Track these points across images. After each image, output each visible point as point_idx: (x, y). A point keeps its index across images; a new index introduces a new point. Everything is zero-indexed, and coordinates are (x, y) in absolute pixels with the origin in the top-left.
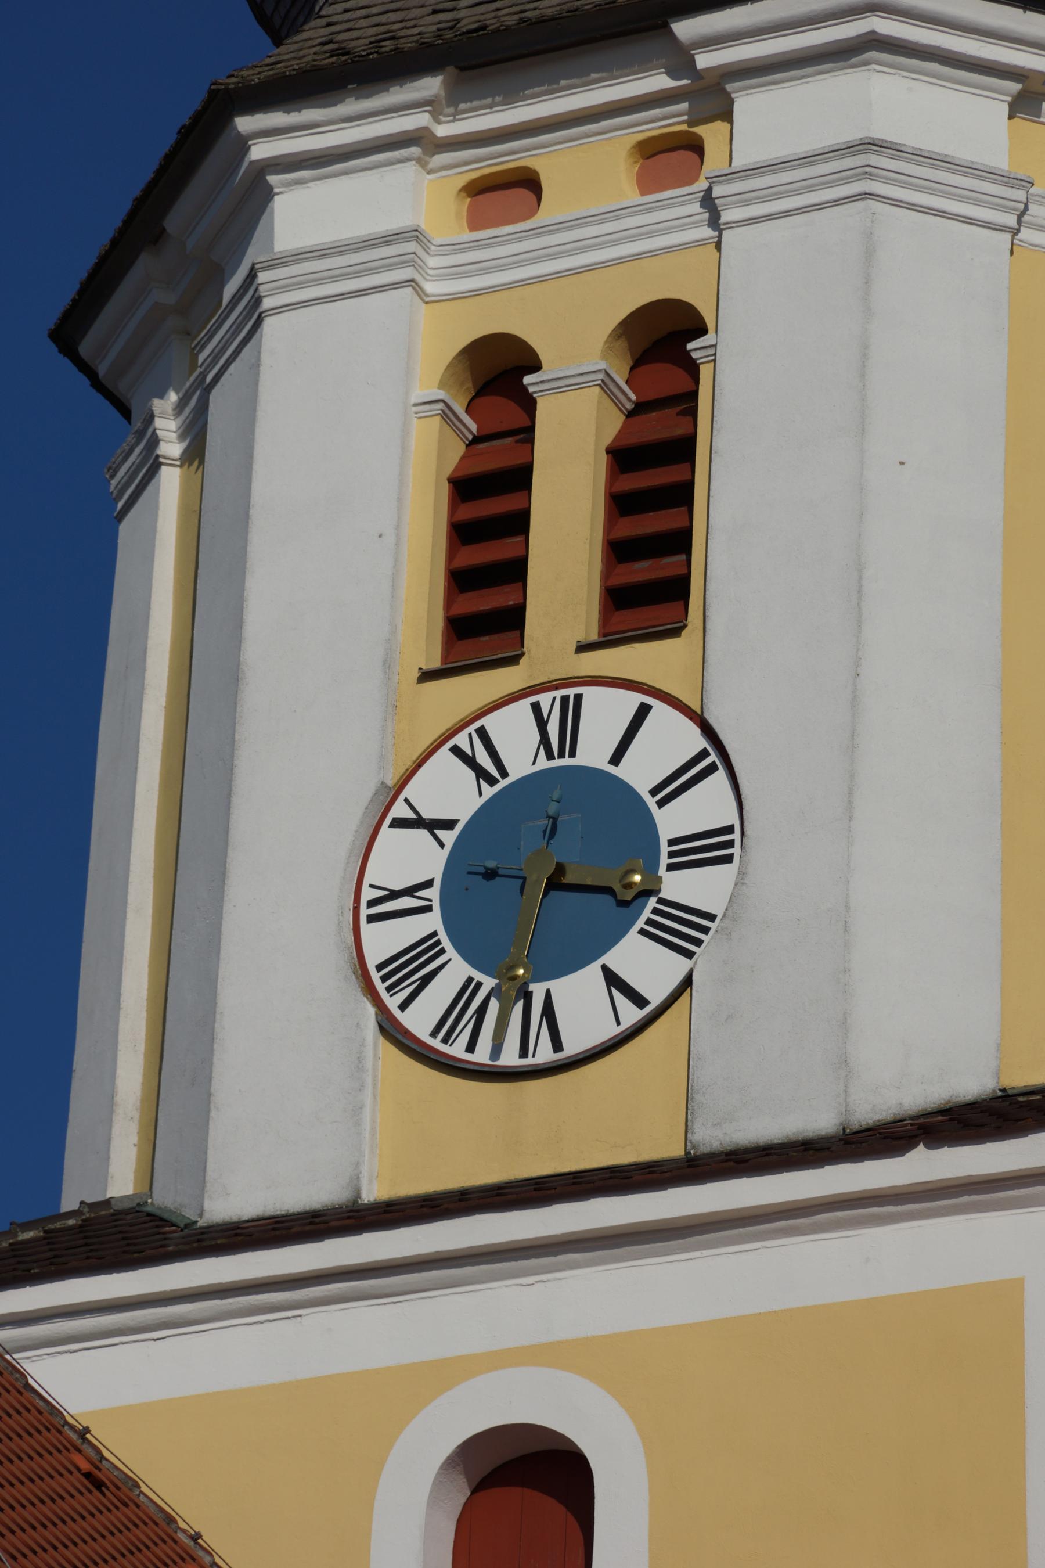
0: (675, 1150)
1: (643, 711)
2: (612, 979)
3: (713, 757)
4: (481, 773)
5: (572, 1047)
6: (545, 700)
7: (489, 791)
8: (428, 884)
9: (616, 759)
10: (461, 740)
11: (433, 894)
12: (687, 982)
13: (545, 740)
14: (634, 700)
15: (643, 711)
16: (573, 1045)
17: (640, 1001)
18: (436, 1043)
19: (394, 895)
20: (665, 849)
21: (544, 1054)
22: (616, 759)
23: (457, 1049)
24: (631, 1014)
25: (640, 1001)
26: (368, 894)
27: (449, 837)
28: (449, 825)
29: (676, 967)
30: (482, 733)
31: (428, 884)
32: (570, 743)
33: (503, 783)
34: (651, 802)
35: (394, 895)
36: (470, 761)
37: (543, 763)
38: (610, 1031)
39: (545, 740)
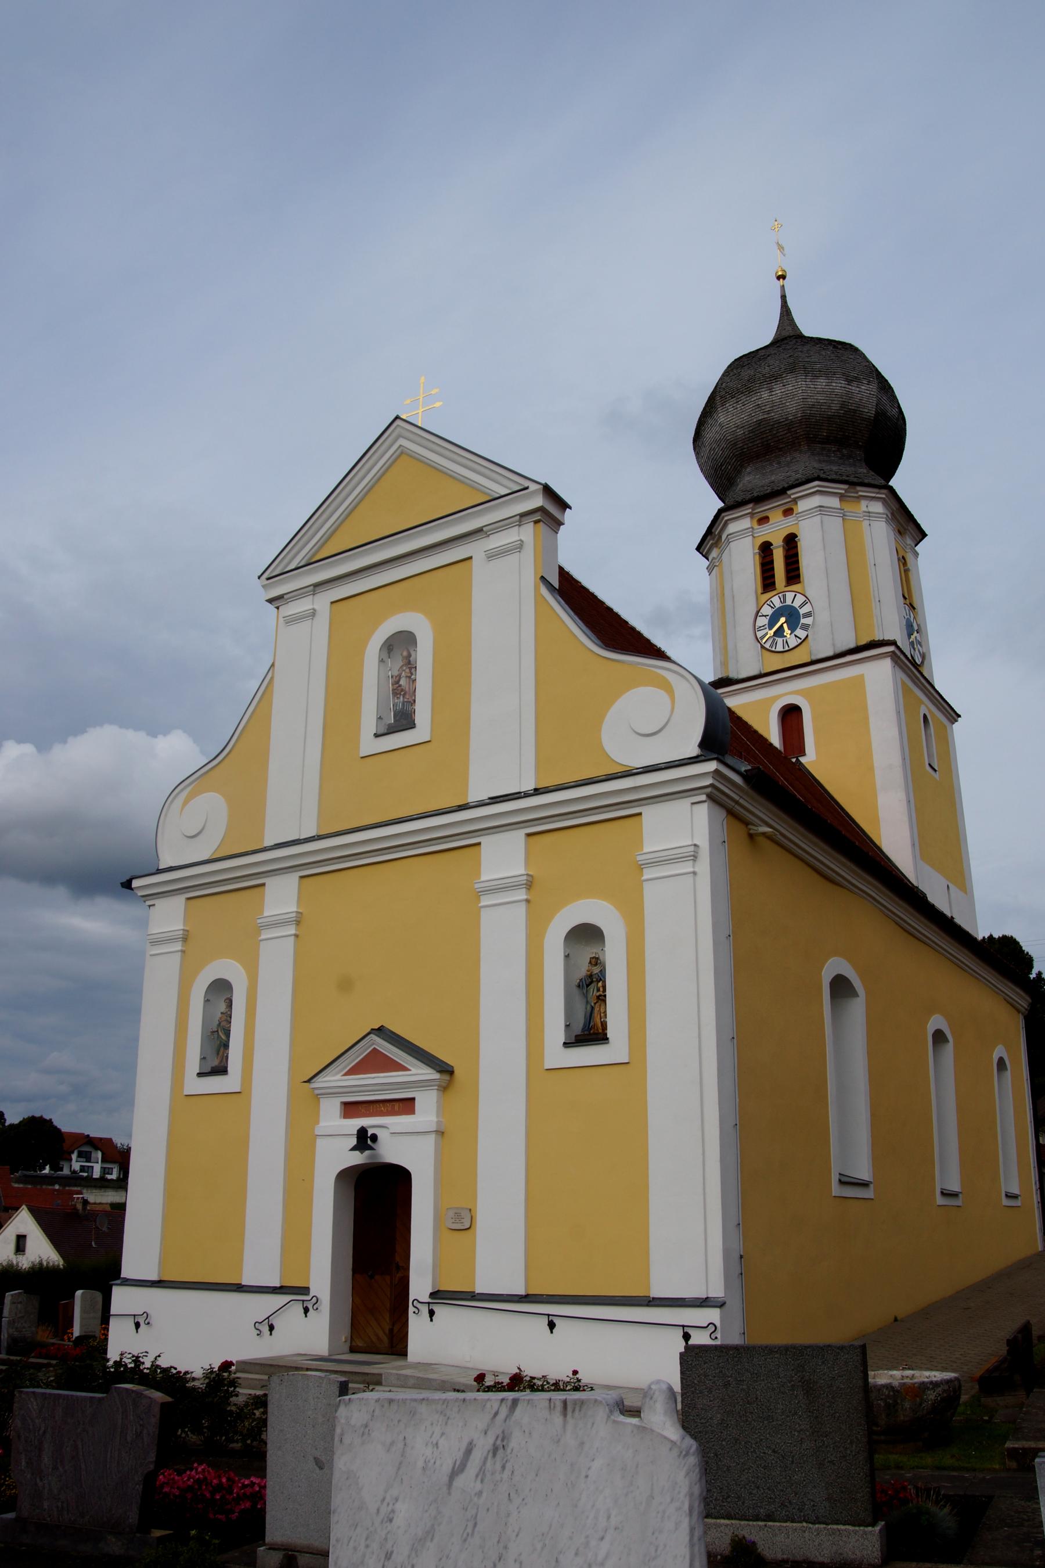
0: (809, 660)
1: (796, 595)
2: (796, 636)
3: (807, 601)
4: (772, 607)
5: (791, 647)
6: (780, 595)
7: (773, 610)
8: (766, 625)
9: (792, 603)
10: (768, 602)
11: (767, 626)
12: (807, 636)
13: (781, 601)
14: (794, 594)
15: (796, 595)
16: (791, 647)
17: (800, 639)
18: (770, 648)
19: (760, 627)
20: (801, 616)
21: (787, 648)
22: (792, 603)
23: (773, 649)
24: (800, 641)
25: (800, 639)
26: (756, 627)
27: (768, 617)
28: (768, 616)
29: (806, 633)
30: (771, 601)
31: (766, 625)
32: (785, 601)
33: (775, 609)
34: (798, 609)
35: (760, 627)
36: (770, 606)
37: (781, 605)
38: (796, 644)
39: (781, 601)
